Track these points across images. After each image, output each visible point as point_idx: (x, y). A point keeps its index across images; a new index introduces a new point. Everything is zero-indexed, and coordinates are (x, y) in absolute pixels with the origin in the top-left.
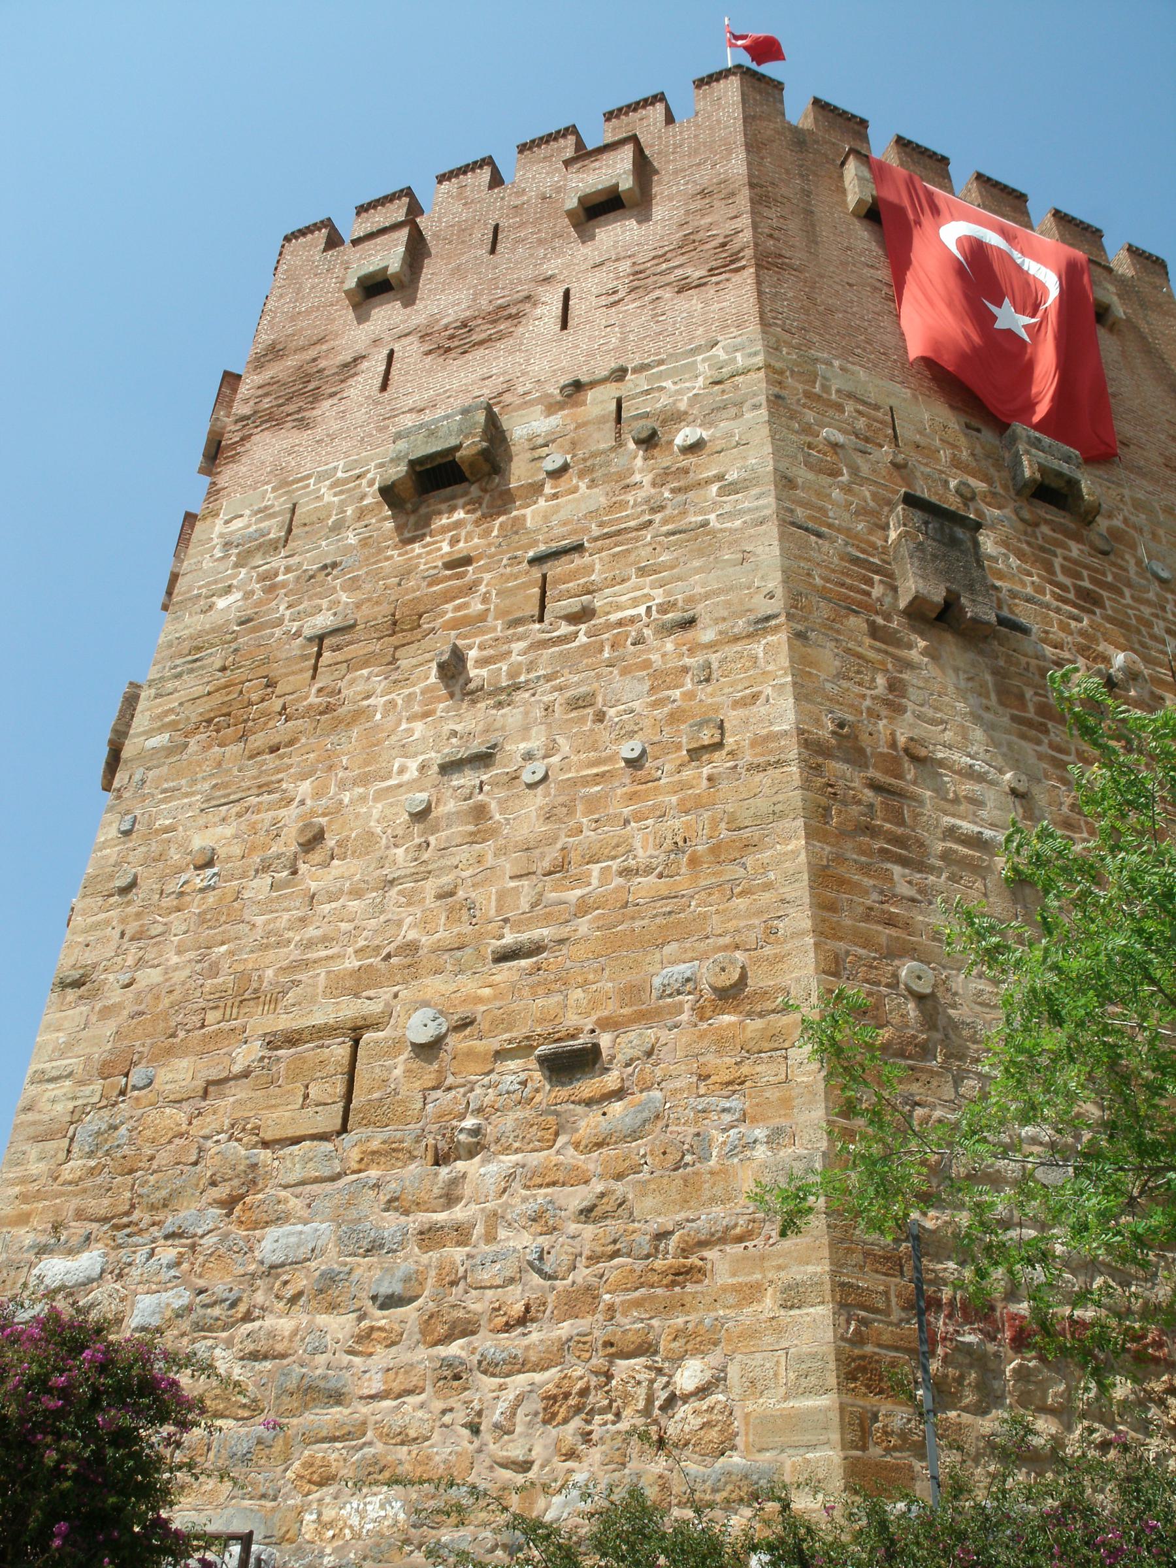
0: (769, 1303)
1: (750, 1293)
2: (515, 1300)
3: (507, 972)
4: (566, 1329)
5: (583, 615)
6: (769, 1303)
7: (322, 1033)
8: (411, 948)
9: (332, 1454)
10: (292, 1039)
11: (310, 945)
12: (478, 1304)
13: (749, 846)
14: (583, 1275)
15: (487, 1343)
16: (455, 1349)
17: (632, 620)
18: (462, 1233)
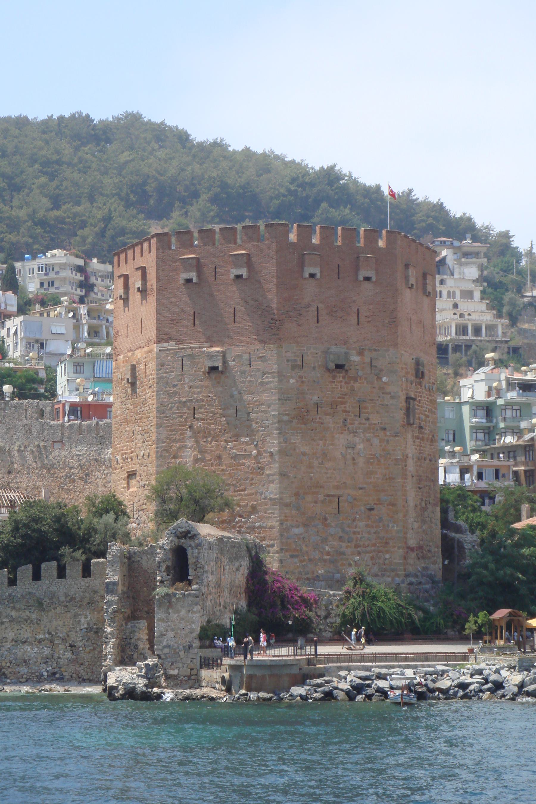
0: (396, 549)
1: (394, 547)
2: (367, 543)
3: (360, 492)
4: (373, 548)
5: (368, 419)
6: (396, 549)
7: (333, 496)
8: (345, 483)
9: (344, 562)
10: (328, 496)
11: (328, 478)
12: (361, 543)
13: (393, 479)
14: (374, 542)
15: (364, 549)
16: (359, 549)
17: (375, 424)
18: (358, 533)
